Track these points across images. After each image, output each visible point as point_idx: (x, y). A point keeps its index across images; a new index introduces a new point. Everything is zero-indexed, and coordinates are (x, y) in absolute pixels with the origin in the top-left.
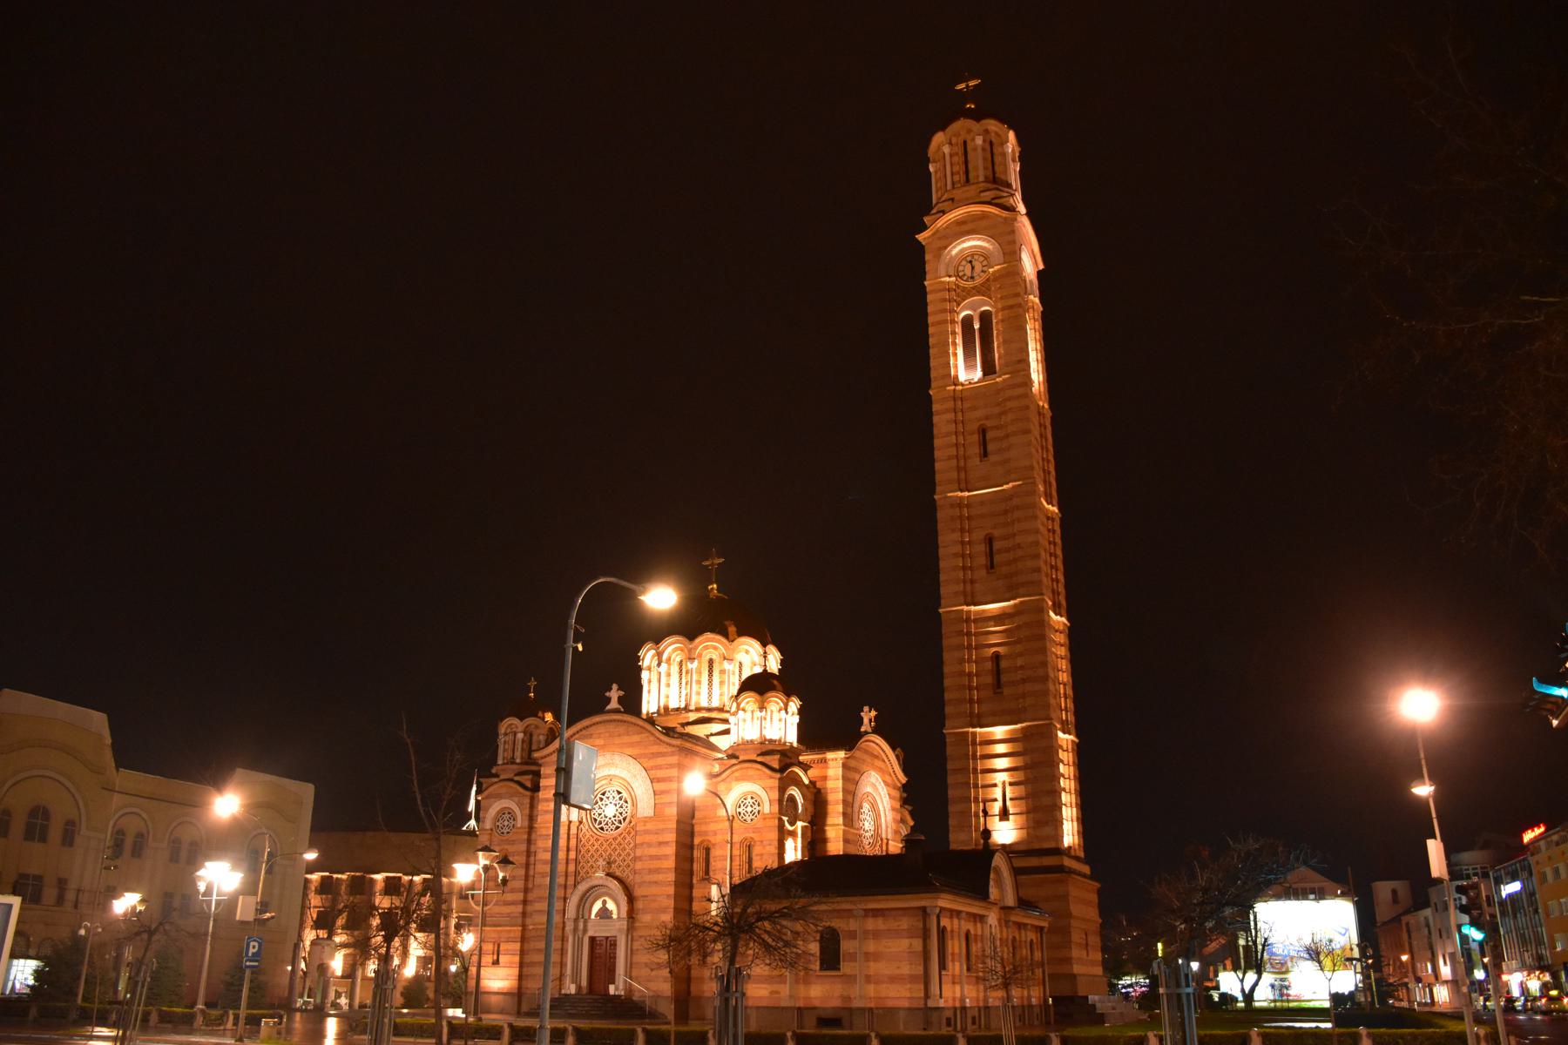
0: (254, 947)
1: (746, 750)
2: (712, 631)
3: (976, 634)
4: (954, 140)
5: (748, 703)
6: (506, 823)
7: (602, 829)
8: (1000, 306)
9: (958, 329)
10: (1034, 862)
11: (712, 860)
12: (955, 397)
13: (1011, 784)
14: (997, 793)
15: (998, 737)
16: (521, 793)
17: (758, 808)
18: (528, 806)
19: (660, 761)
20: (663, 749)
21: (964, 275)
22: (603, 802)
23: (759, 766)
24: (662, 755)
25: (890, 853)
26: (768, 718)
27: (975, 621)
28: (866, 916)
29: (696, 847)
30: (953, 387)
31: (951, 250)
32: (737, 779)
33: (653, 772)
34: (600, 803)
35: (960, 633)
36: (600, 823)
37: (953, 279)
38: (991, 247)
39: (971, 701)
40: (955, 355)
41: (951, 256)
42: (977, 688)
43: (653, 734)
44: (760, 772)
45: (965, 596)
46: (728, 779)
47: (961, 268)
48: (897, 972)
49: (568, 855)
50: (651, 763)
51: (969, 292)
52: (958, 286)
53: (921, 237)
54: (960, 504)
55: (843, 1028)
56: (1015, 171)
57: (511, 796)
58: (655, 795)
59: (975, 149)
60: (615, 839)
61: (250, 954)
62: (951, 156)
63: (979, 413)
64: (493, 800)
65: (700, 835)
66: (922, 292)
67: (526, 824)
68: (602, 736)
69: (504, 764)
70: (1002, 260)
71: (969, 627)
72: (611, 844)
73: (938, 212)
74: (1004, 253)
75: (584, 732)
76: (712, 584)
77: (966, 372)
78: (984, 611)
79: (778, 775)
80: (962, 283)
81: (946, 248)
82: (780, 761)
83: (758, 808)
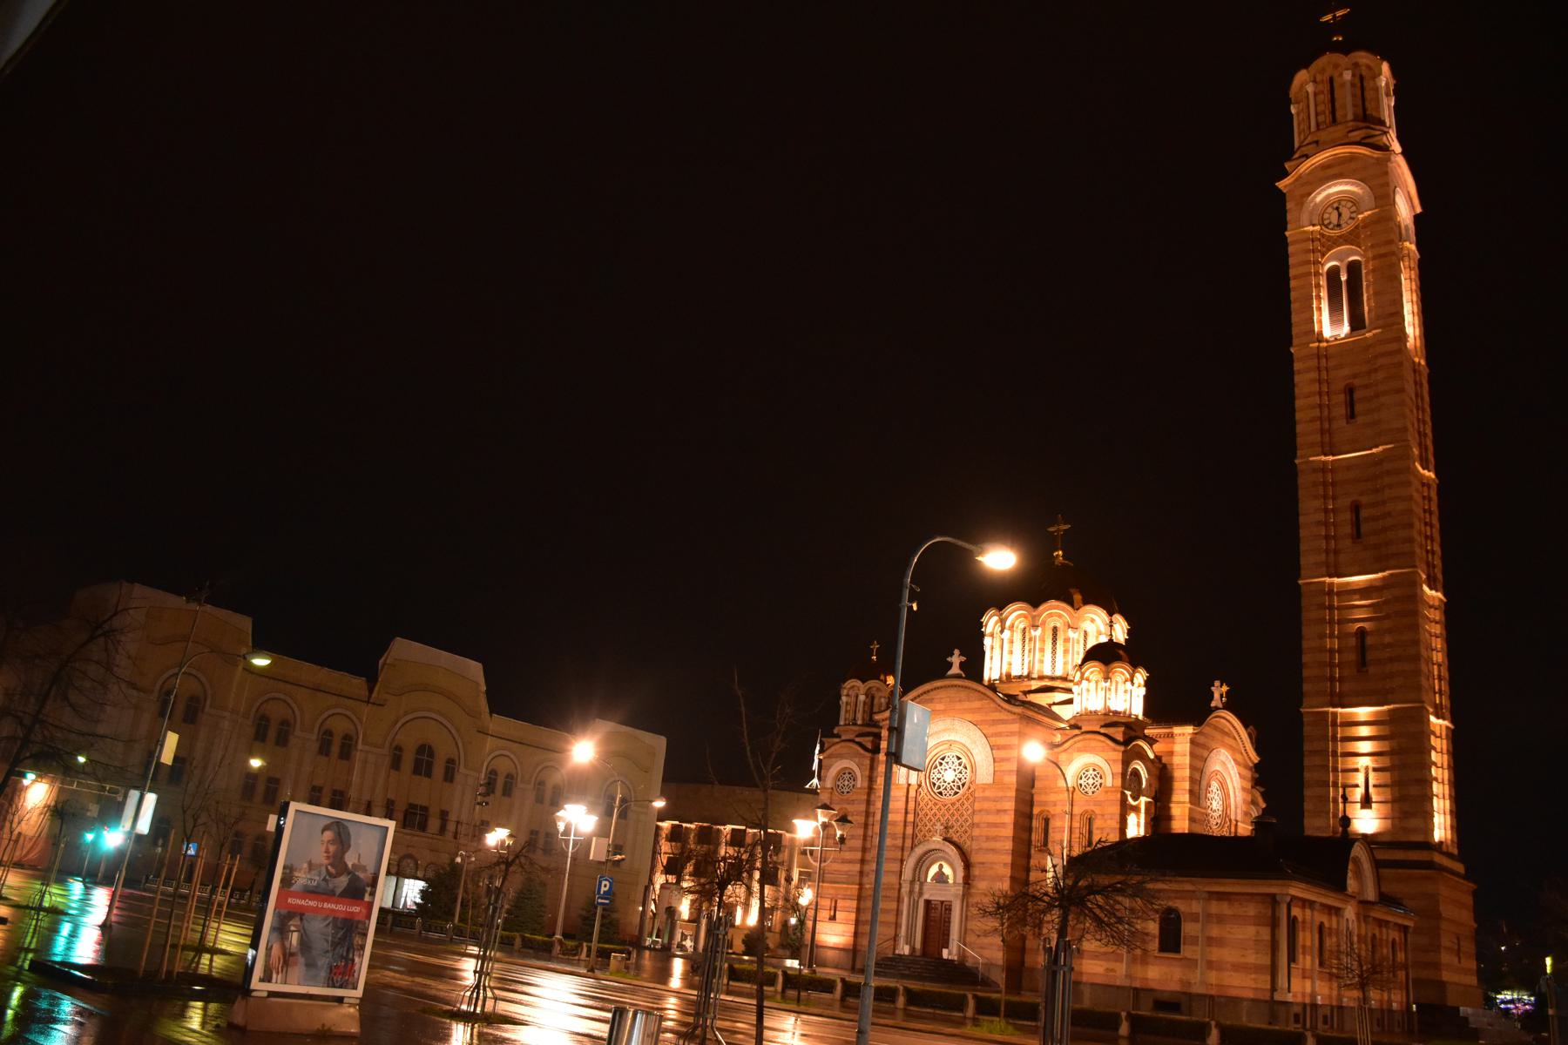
0: (605, 886)
1: (1089, 720)
2: (1058, 598)
3: (1339, 608)
4: (1319, 78)
5: (1092, 673)
6: (846, 783)
7: (941, 793)
8: (1370, 254)
9: (1323, 282)
10: (1399, 855)
11: (1050, 831)
12: (1319, 355)
13: (1375, 770)
14: (1359, 778)
15: (1362, 719)
16: (861, 754)
17: (1100, 781)
18: (868, 767)
19: (1001, 728)
20: (1003, 716)
21: (1330, 223)
22: (942, 767)
23: (1102, 738)
25: (1238, 835)
26: (1113, 688)
27: (1339, 594)
28: (1209, 899)
29: (1035, 817)
30: (1317, 344)
31: (1315, 197)
32: (1080, 750)
33: (994, 739)
34: (939, 768)
35: (1322, 606)
36: (939, 787)
37: (1318, 228)
38: (1360, 192)
39: (1332, 679)
40: (1319, 309)
41: (1316, 204)
42: (1339, 665)
43: (994, 701)
44: (1104, 744)
45: (1328, 567)
46: (1069, 751)
47: (1326, 216)
48: (1243, 960)
49: (906, 817)
50: (992, 730)
51: (1335, 242)
52: (1323, 236)
53: (1281, 184)
54: (1323, 468)
55: (1181, 1014)
56: (1389, 106)
58: (994, 762)
59: (1343, 85)
60: (953, 804)
61: (602, 893)
62: (1316, 94)
63: (1346, 372)
64: (833, 760)
65: (1040, 806)
66: (1284, 242)
67: (866, 784)
68: (943, 700)
69: (845, 725)
70: (1373, 204)
71: (1331, 600)
72: (949, 809)
73: (1300, 157)
74: (1375, 198)
75: (925, 696)
76: (1057, 550)
77: (1330, 327)
78: (1348, 584)
79: (1122, 748)
80: (1328, 232)
81: (1310, 194)
82: (1124, 733)
83: (1100, 781)
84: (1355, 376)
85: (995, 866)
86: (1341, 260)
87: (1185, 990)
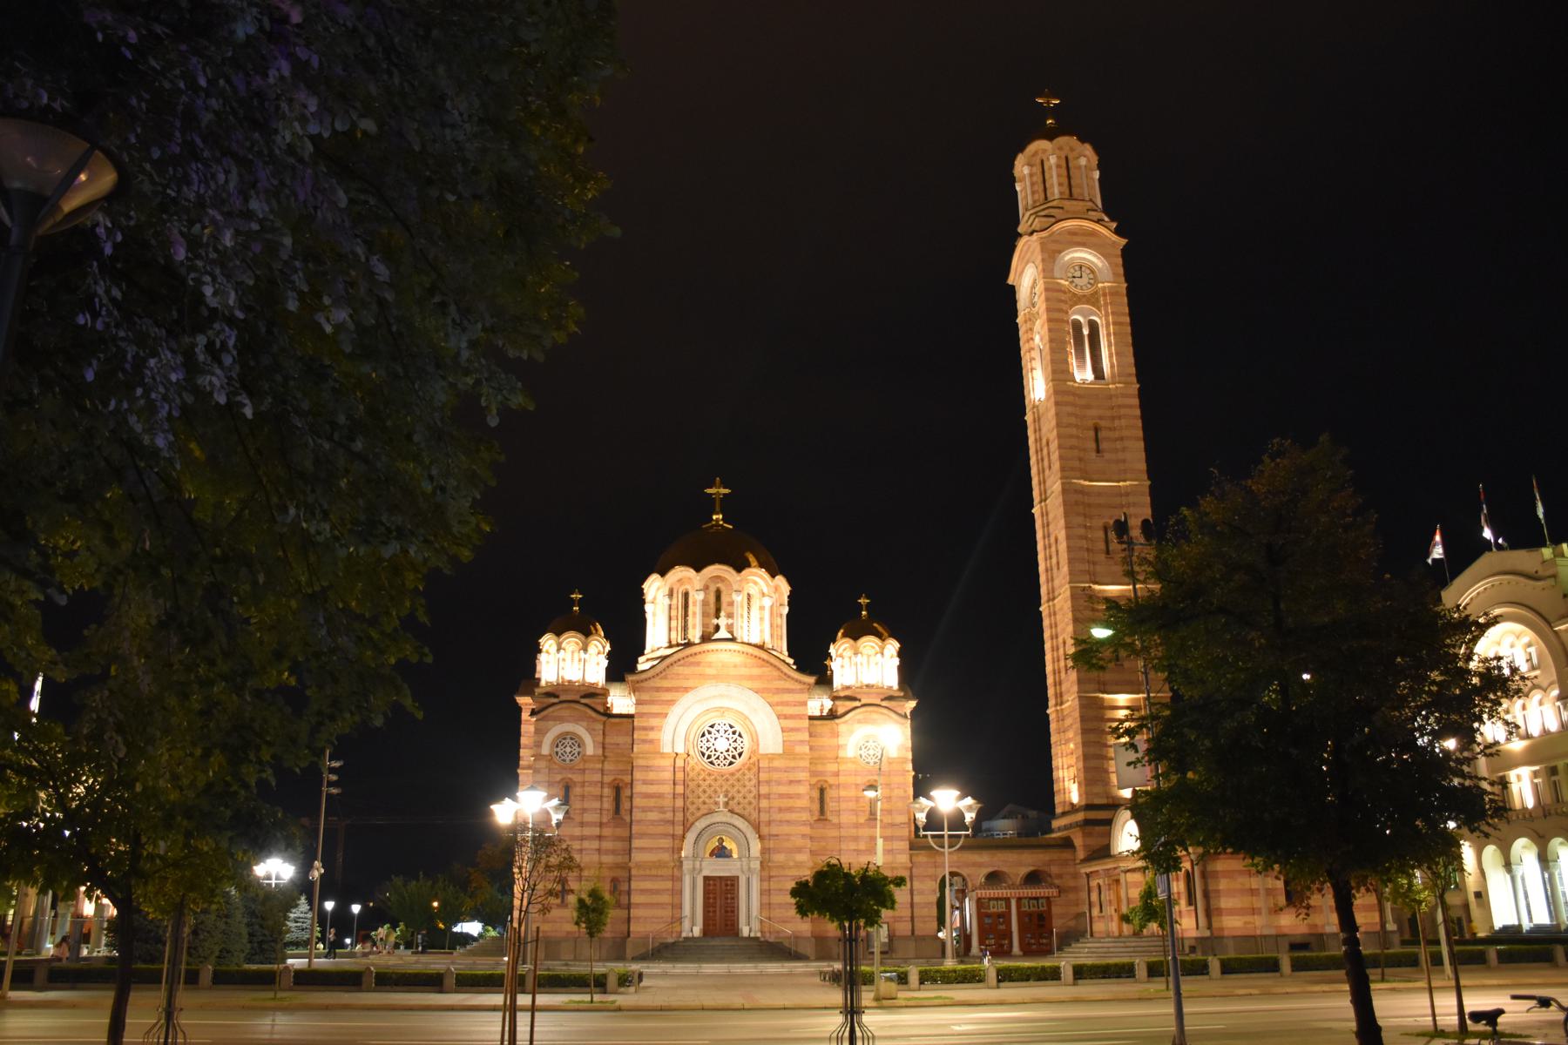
5: (845, 650)
16: (591, 717)
18: (601, 732)
19: (787, 697)
22: (731, 735)
24: (789, 691)
31: (1064, 256)
32: (859, 722)
50: (777, 698)
55: (1312, 951)
57: (576, 720)
59: (1079, 167)
60: (732, 774)
63: (1093, 412)
64: (551, 723)
67: (600, 752)
78: (1104, 591)
81: (1060, 252)
84: (1101, 418)
85: (792, 838)
86: (1084, 317)
87: (1313, 931)
